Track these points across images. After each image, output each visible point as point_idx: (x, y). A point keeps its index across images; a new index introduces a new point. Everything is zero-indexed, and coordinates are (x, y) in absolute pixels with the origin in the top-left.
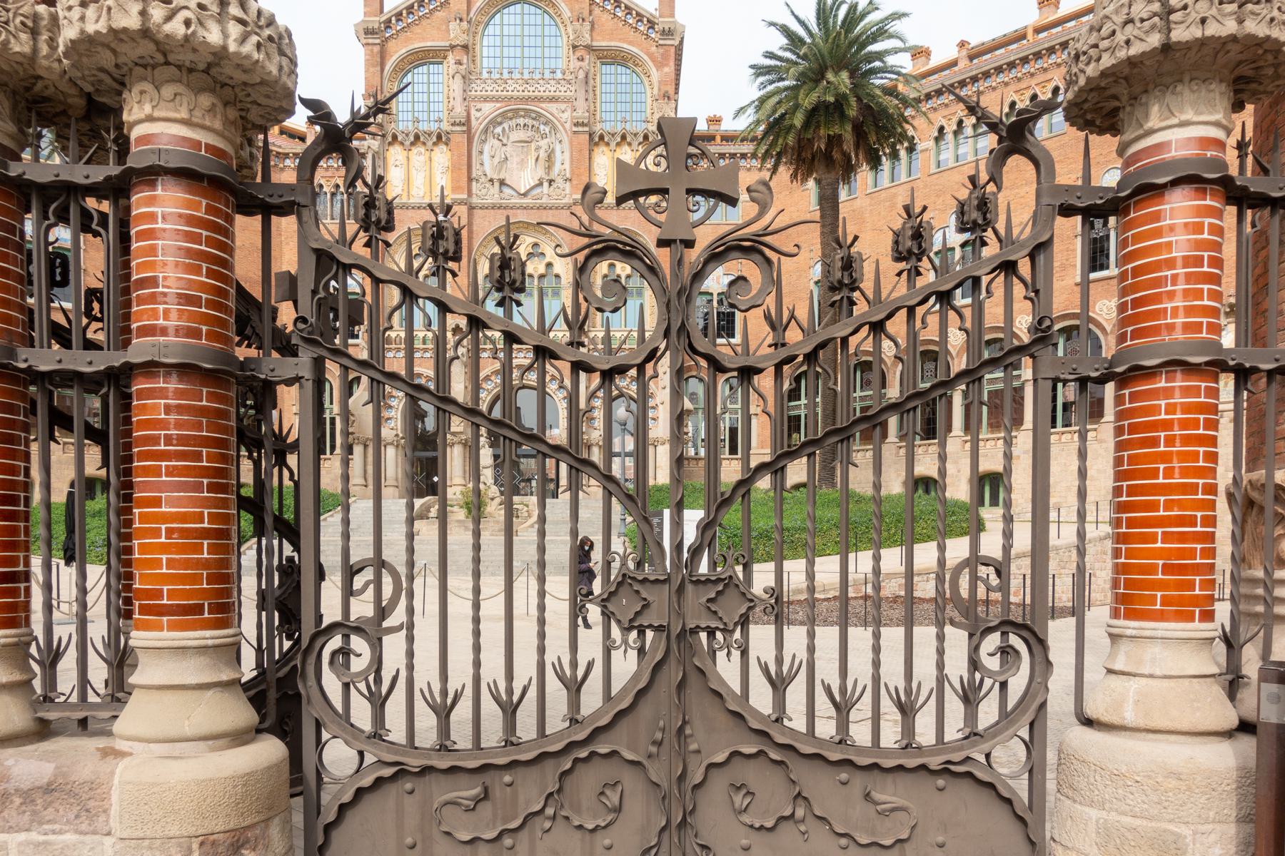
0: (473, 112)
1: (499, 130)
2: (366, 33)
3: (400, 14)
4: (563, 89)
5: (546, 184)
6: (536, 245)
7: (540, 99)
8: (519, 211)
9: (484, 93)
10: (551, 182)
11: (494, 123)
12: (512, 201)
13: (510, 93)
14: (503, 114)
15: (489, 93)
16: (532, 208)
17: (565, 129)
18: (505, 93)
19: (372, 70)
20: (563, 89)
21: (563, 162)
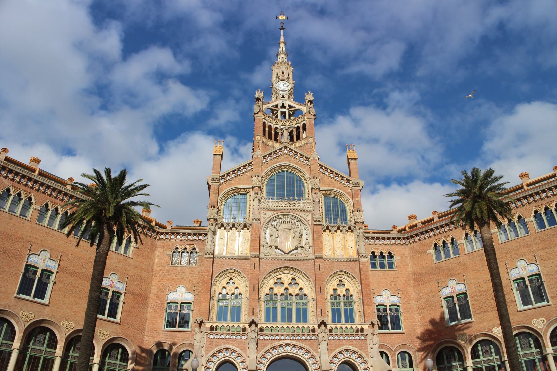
0: (262, 215)
1: (275, 223)
2: (212, 180)
3: (229, 173)
4: (307, 206)
5: (299, 249)
6: (293, 279)
7: (296, 210)
8: (285, 261)
9: (268, 207)
10: (302, 247)
11: (273, 220)
12: (282, 256)
13: (281, 207)
14: (277, 217)
15: (270, 207)
16: (292, 260)
17: (308, 224)
19: (214, 195)
20: (307, 206)
21: (307, 238)
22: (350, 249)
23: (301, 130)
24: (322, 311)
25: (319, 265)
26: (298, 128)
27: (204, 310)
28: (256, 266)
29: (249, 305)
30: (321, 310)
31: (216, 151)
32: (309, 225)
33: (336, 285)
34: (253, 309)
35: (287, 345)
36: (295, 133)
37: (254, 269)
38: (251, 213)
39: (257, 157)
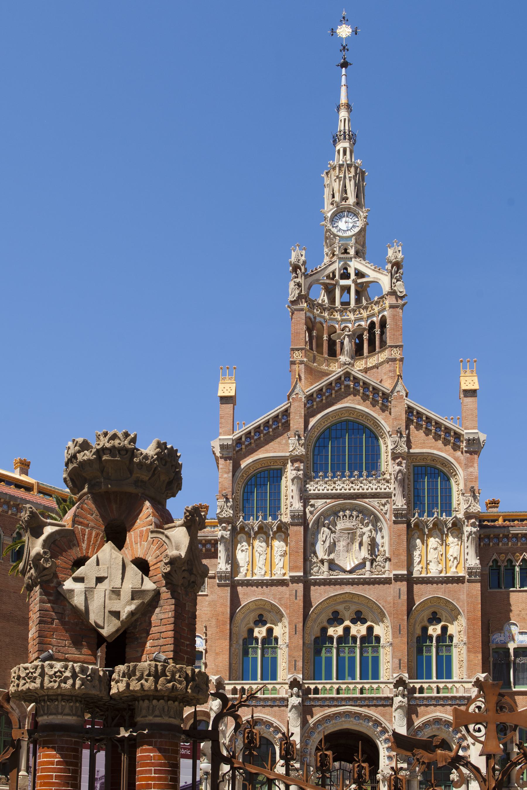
5: (368, 564)
7: (363, 496)
13: (338, 491)
18: (334, 491)
22: (452, 560)
23: (377, 331)
24: (402, 661)
25: (400, 590)
26: (373, 324)
27: (221, 664)
28: (298, 594)
29: (290, 656)
30: (400, 660)
31: (225, 390)
32: (386, 521)
33: (426, 620)
34: (295, 661)
35: (347, 714)
36: (366, 336)
37: (296, 599)
38: (288, 502)
39: (297, 397)
